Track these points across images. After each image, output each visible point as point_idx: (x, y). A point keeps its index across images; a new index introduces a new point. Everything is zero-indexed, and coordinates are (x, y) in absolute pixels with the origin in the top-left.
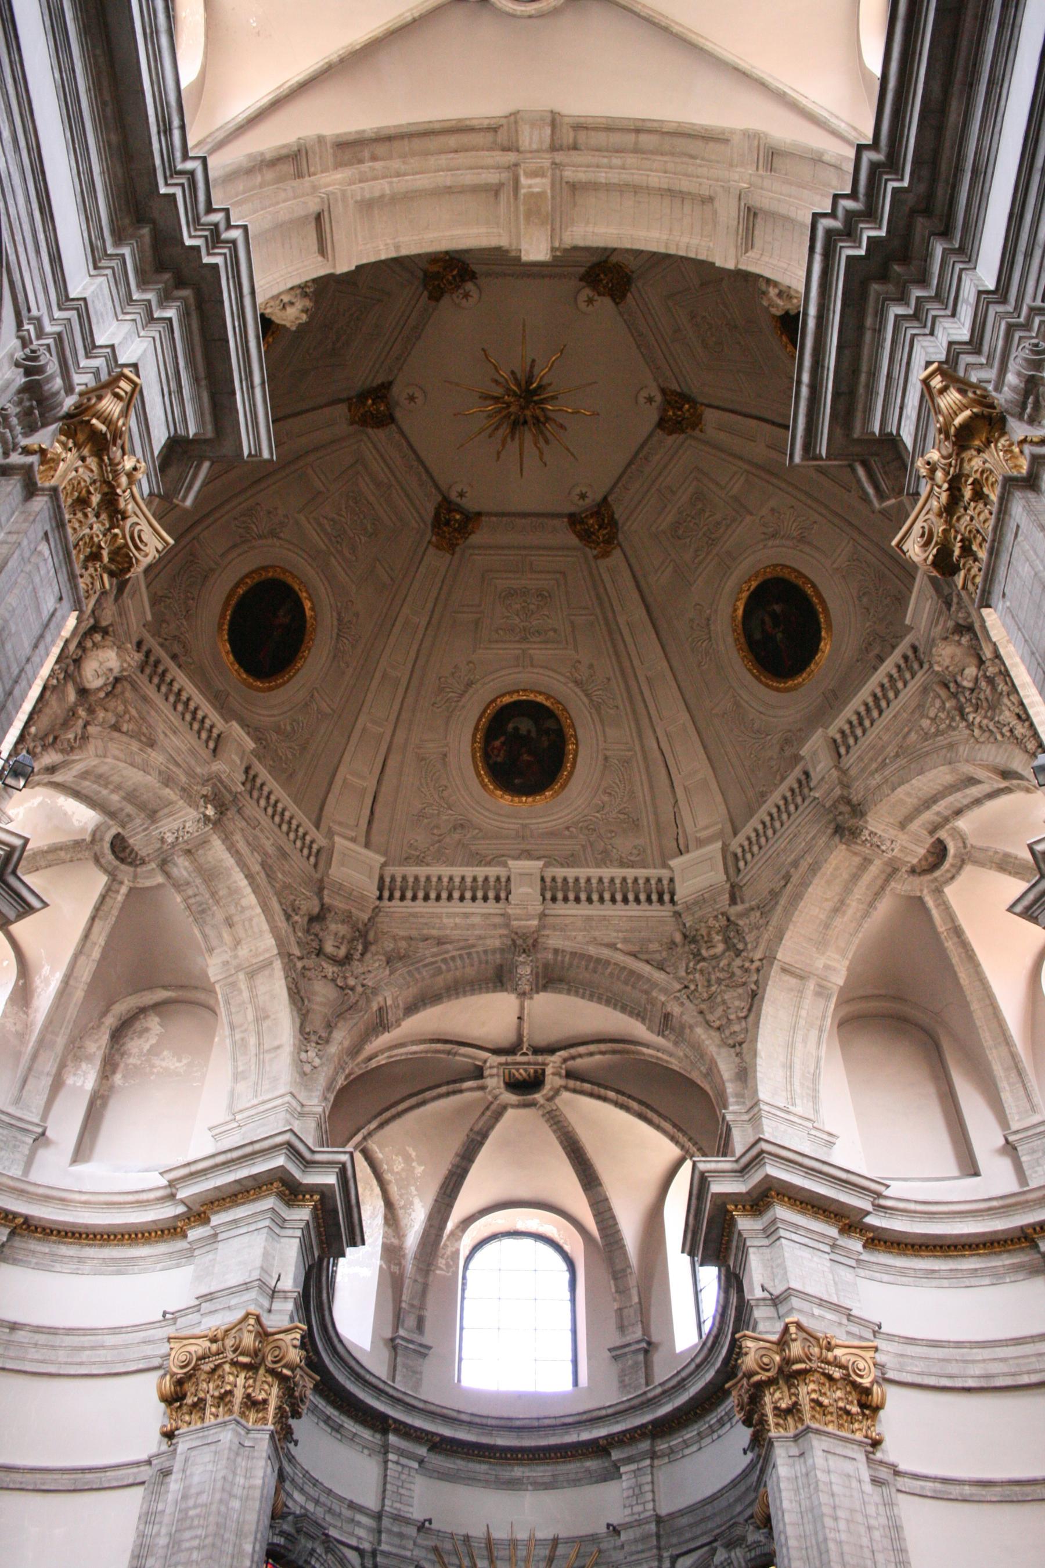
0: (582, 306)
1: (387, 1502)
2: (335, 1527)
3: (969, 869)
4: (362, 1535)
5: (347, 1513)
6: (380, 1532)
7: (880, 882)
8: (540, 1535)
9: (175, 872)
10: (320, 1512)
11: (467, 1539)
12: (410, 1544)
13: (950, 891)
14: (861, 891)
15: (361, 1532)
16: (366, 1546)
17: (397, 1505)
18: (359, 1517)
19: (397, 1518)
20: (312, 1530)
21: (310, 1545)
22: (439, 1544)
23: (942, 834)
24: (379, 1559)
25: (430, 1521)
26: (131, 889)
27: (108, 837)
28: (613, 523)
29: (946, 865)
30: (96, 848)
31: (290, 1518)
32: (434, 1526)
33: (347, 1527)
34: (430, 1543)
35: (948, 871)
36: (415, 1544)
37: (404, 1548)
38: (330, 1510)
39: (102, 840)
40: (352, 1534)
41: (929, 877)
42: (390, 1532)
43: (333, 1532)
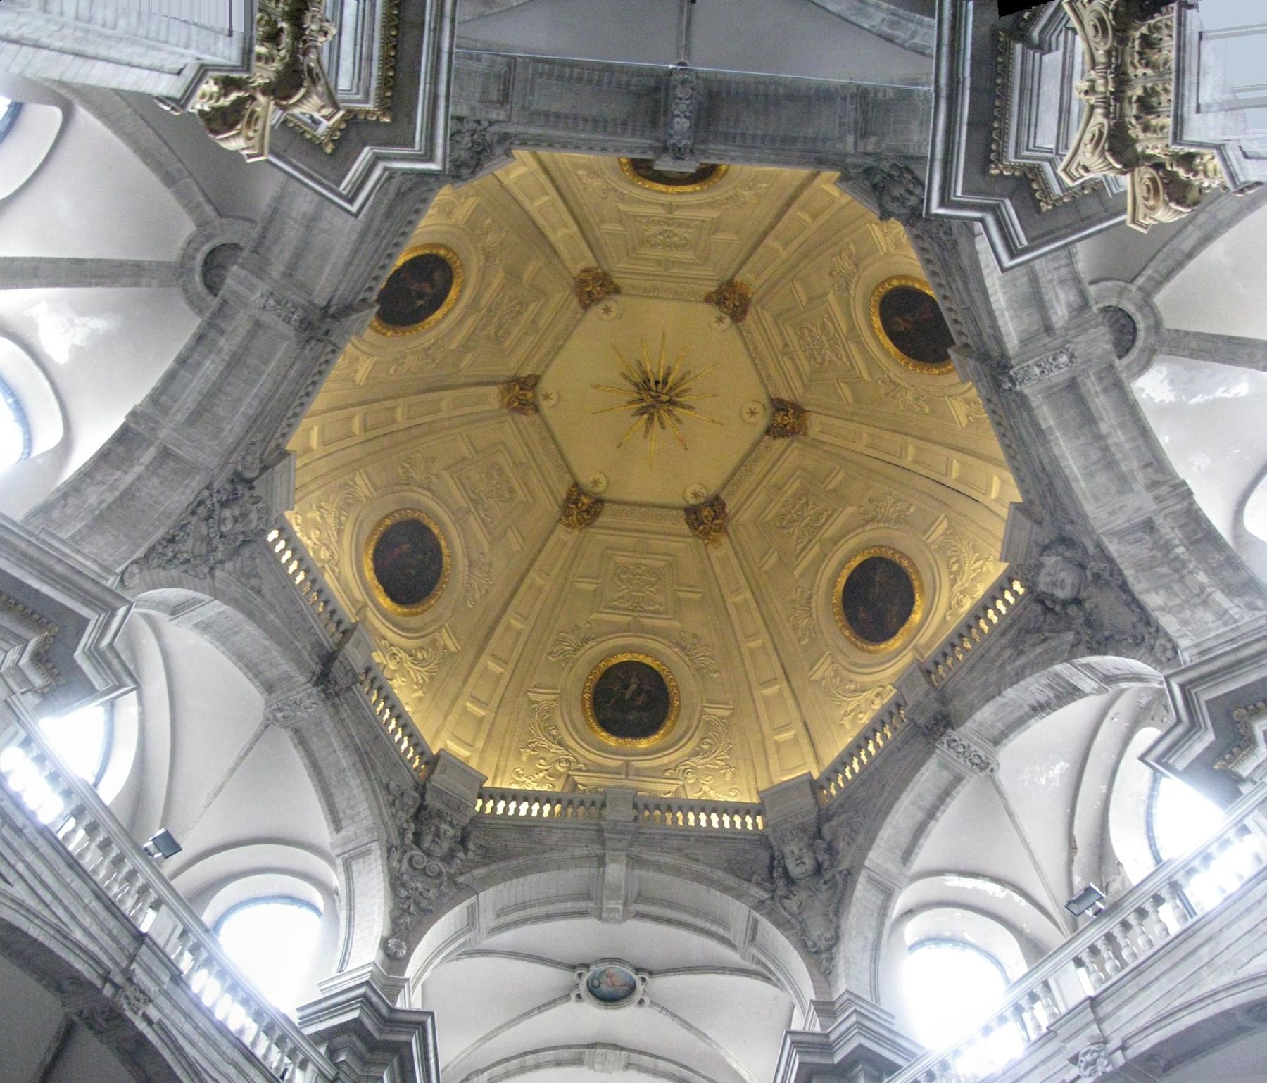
0: (603, 479)
3: (173, 256)
7: (270, 235)
9: (1073, 297)
13: (189, 227)
14: (292, 234)
23: (214, 303)
26: (1132, 281)
27: (1134, 352)
28: (579, 295)
29: (200, 257)
30: (1152, 340)
35: (197, 250)
39: (1142, 351)
41: (216, 242)
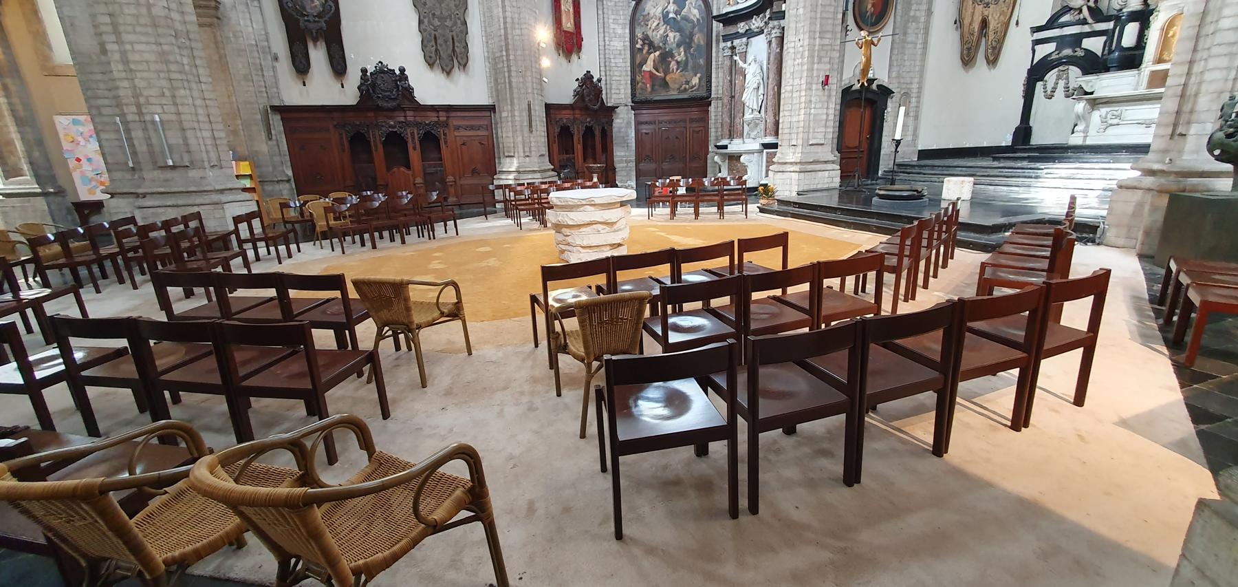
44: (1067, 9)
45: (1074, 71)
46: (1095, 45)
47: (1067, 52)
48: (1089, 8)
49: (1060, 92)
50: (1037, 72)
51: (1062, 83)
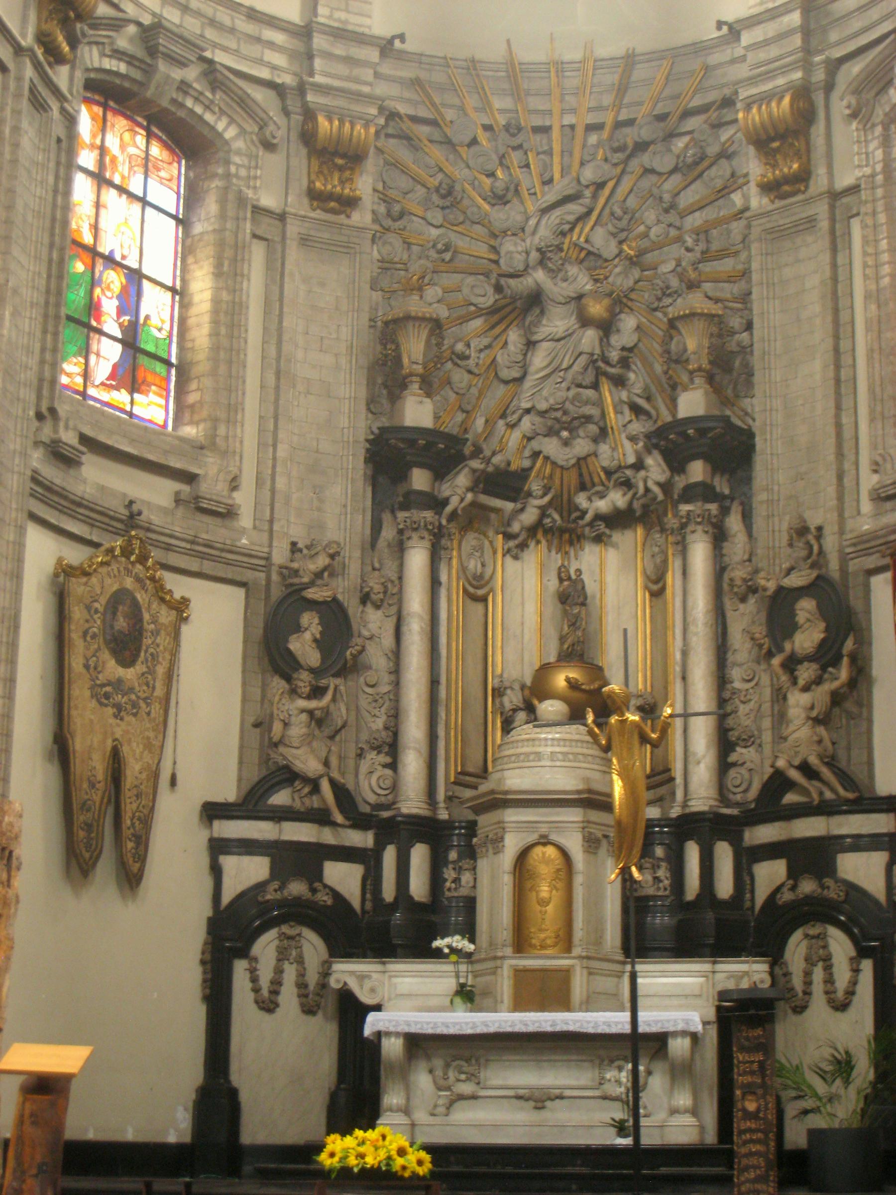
1: (321, 10)
2: (225, 49)
4: (277, 64)
5: (249, 28)
6: (310, 57)
8: (602, 52)
10: (192, 26)
11: (473, 65)
12: (367, 74)
15: (280, 60)
16: (288, 79)
17: (343, 15)
18: (270, 34)
19: (340, 34)
20: (177, 49)
21: (177, 74)
22: (423, 75)
24: (310, 98)
25: (402, 37)
31: (132, 29)
32: (410, 46)
33: (254, 50)
34: (407, 72)
36: (377, 75)
37: (357, 81)
38: (212, 22)
40: (260, 62)
42: (328, 56)
43: (220, 57)
44: (288, 776)
45: (313, 946)
46: (344, 878)
47: (297, 888)
48: (333, 783)
49: (289, 996)
50: (230, 933)
51: (290, 973)
